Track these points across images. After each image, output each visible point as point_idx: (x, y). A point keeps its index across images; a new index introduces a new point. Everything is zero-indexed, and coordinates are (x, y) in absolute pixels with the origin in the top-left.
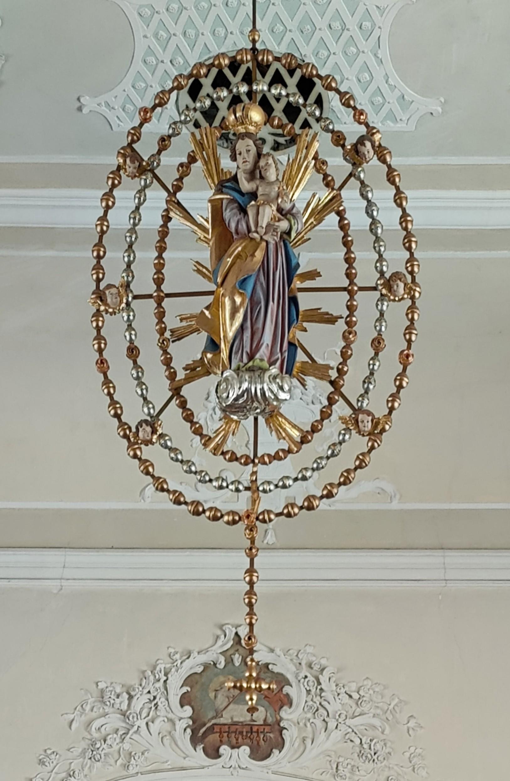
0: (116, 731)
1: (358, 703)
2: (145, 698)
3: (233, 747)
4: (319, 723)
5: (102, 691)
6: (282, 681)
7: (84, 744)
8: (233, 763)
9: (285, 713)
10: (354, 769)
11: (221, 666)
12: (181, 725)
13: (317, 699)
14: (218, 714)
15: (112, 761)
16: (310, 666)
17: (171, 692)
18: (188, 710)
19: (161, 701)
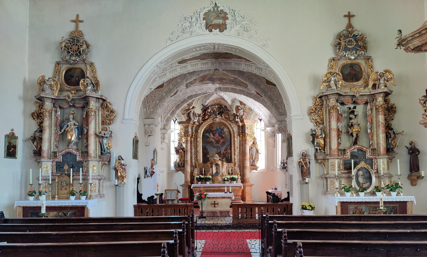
0: (189, 26)
1: (244, 18)
2: (195, 19)
3: (215, 29)
4: (235, 23)
5: (185, 17)
6: (226, 14)
7: (181, 30)
8: (215, 33)
9: (227, 21)
10: (243, 34)
11: (212, 11)
12: (203, 25)
13: (234, 18)
14: (212, 22)
15: (188, 34)
16: (232, 10)
17: (201, 17)
18: (205, 21)
19: (199, 19)
